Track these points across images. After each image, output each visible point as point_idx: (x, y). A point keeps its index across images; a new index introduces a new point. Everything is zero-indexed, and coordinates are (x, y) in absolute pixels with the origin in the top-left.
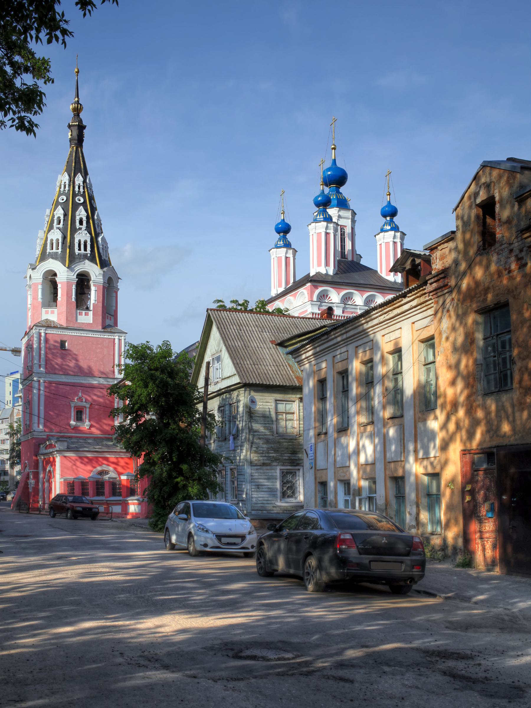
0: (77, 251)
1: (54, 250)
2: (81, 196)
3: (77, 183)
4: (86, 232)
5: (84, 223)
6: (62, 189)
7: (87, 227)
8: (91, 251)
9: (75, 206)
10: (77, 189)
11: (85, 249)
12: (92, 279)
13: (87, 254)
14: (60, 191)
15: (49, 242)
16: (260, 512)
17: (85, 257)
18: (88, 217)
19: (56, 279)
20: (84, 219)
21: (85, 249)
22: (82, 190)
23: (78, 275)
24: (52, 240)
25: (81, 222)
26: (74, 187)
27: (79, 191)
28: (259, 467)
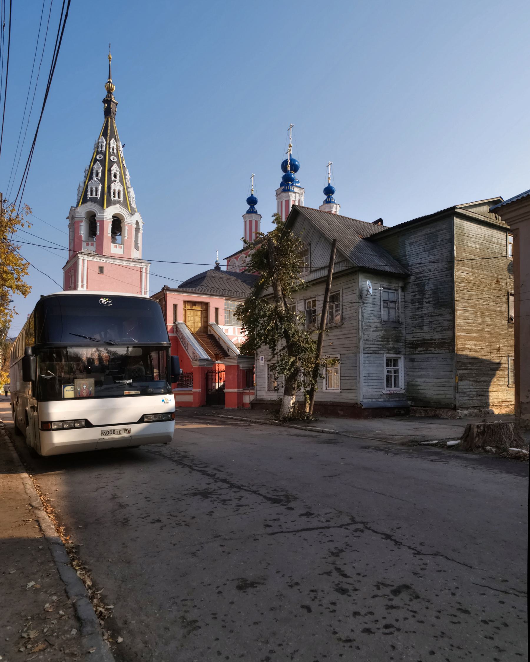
0: (112, 198)
1: (94, 196)
2: (115, 156)
3: (111, 146)
4: (119, 184)
5: (118, 177)
6: (100, 149)
7: (120, 180)
8: (123, 199)
9: (111, 163)
10: (111, 150)
11: (119, 197)
12: (126, 220)
13: (120, 201)
14: (97, 151)
15: (89, 189)
16: (370, 400)
17: (119, 202)
18: (120, 173)
19: (96, 218)
20: (118, 173)
21: (119, 197)
22: (115, 151)
23: (113, 217)
24: (91, 188)
25: (115, 176)
26: (110, 148)
27: (113, 152)
28: (369, 355)
